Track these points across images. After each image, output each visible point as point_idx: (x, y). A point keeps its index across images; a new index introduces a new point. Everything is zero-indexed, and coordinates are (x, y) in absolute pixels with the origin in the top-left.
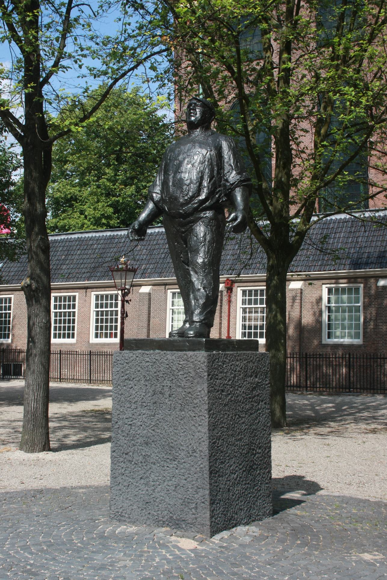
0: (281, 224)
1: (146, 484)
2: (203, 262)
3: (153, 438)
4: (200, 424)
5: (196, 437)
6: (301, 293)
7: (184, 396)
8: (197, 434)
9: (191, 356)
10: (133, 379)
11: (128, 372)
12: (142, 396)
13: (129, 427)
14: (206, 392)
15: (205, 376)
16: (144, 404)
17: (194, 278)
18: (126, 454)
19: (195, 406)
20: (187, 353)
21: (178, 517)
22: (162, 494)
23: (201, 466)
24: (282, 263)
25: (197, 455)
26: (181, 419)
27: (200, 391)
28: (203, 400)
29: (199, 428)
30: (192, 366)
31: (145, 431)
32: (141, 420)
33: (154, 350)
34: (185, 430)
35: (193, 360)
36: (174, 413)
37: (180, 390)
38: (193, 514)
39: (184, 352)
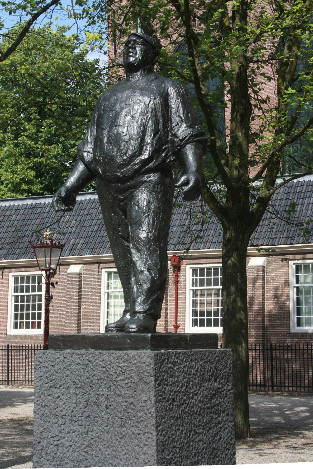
0: (239, 189)
2: (147, 237)
4: (146, 443)
6: (264, 271)
7: (125, 408)
8: (142, 456)
9: (133, 357)
10: (61, 386)
11: (54, 377)
12: (72, 408)
14: (153, 402)
15: (151, 381)
16: (75, 419)
17: (136, 257)
19: (140, 420)
20: (129, 352)
24: (241, 236)
26: (122, 438)
27: (145, 401)
28: (150, 413)
29: (145, 449)
30: (134, 368)
31: (76, 454)
32: (70, 439)
33: (86, 348)
34: (126, 451)
35: (135, 361)
36: (112, 429)
37: (120, 399)
39: (125, 351)
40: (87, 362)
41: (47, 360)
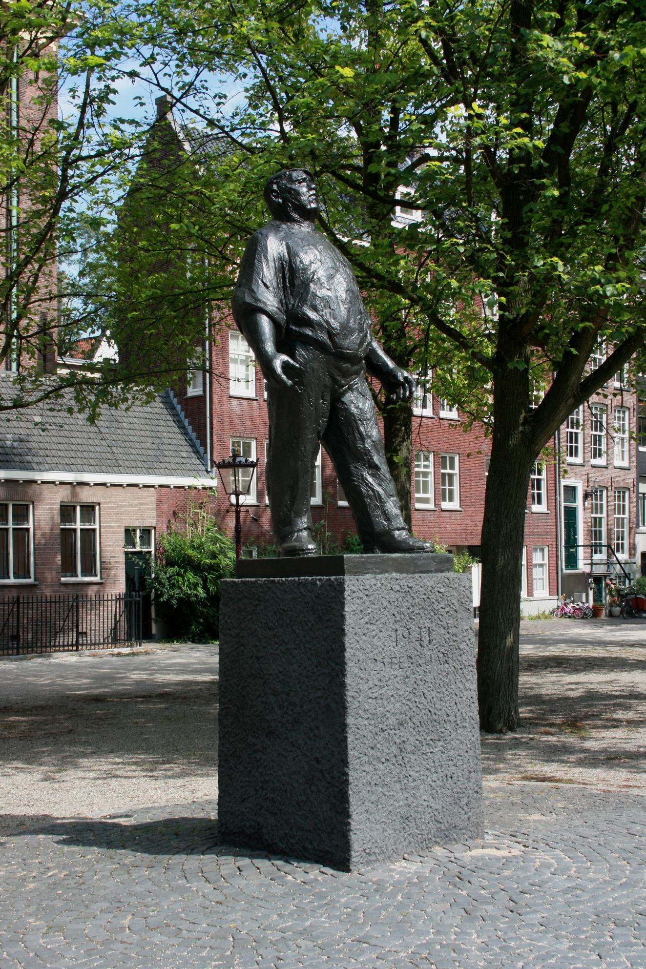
1: (404, 789)
3: (410, 713)
5: (464, 698)
11: (370, 610)
13: (374, 701)
18: (372, 748)
21: (447, 826)
22: (426, 798)
23: (473, 739)
25: (467, 725)
27: (467, 630)
37: (443, 631)
38: (466, 813)
40: (407, 589)
41: (361, 588)
